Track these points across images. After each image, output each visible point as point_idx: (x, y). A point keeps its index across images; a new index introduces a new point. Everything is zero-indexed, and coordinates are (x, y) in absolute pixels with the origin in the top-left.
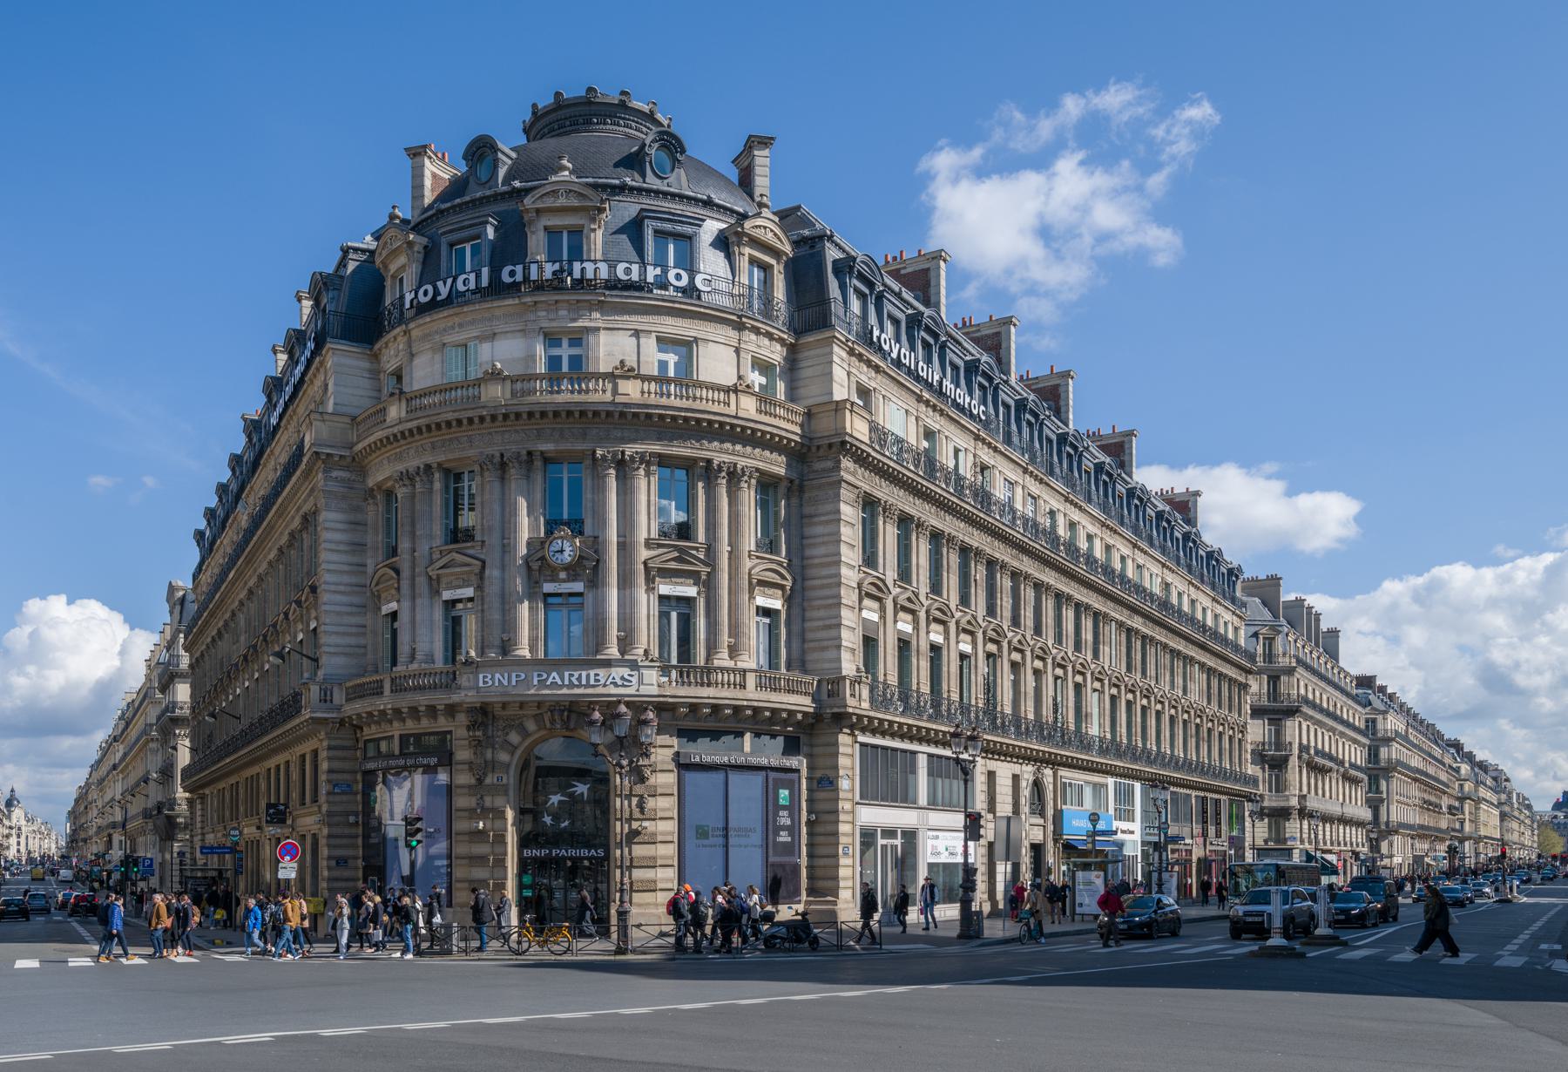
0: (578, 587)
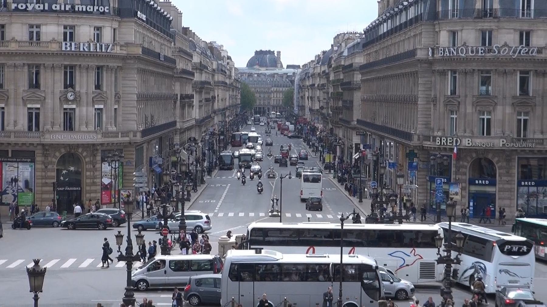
0: (74, 106)
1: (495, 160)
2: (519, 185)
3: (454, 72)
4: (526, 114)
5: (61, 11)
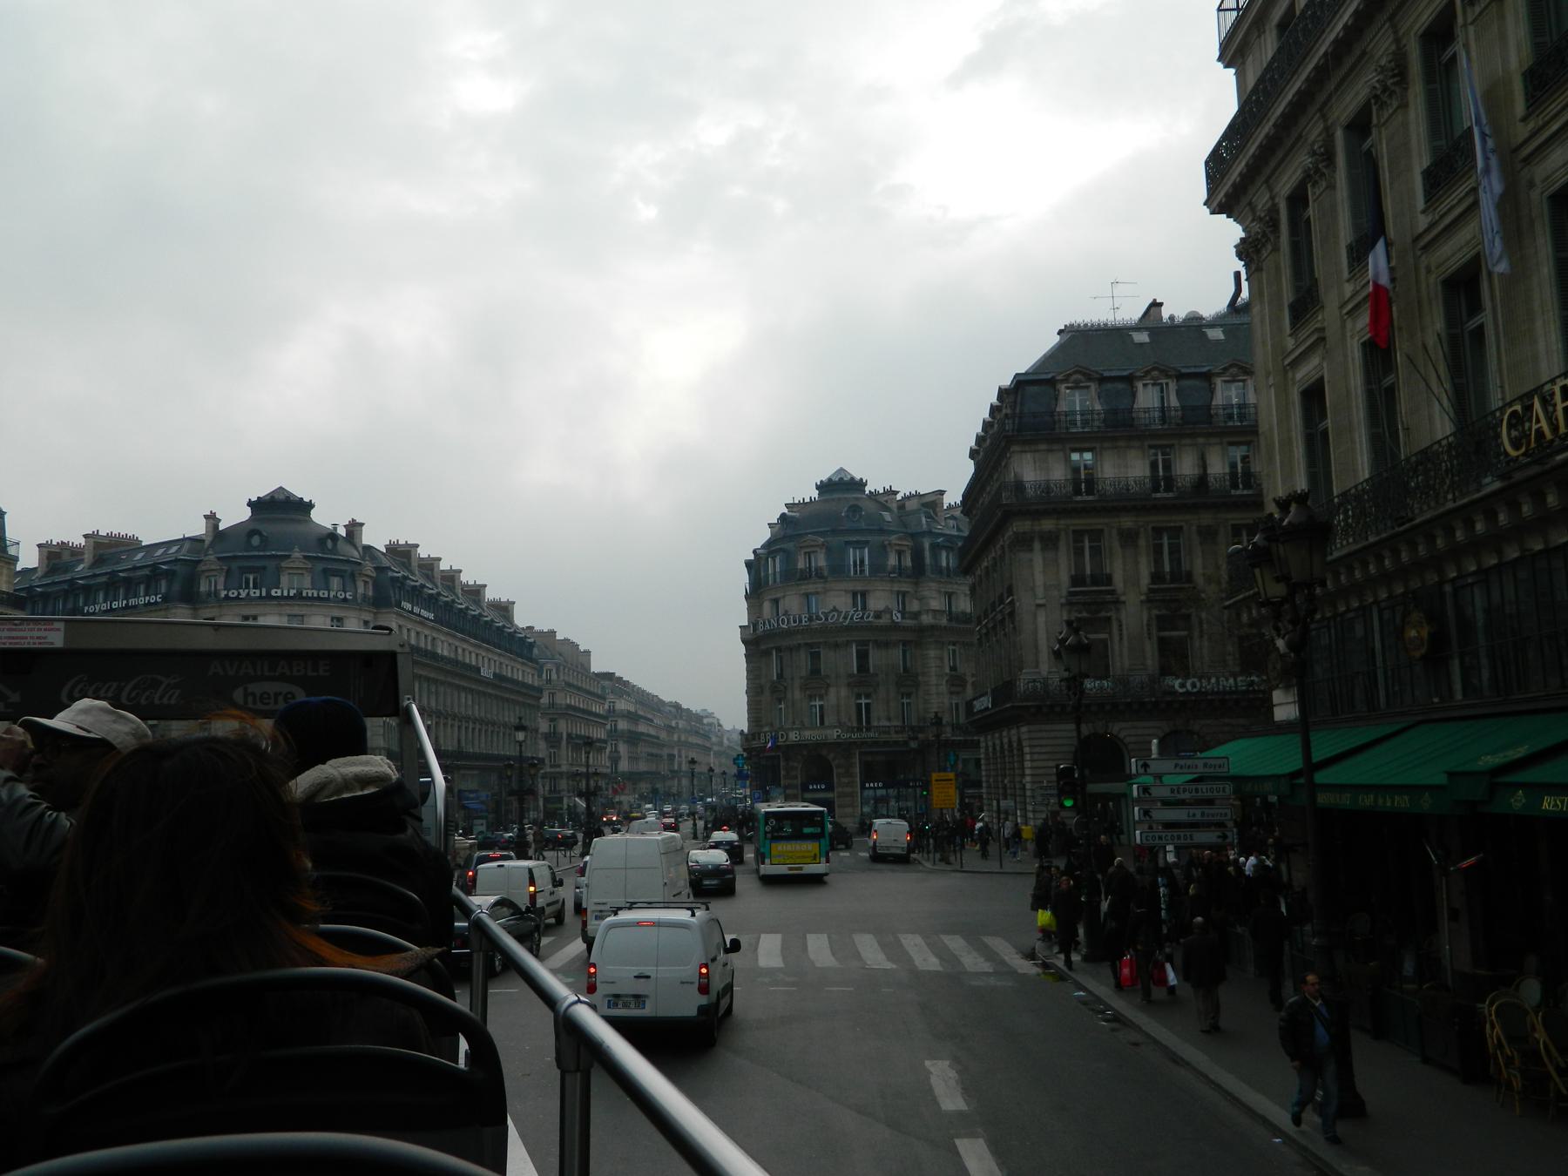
1: (831, 757)
2: (863, 788)
3: (779, 649)
4: (867, 696)
5: (282, 597)
